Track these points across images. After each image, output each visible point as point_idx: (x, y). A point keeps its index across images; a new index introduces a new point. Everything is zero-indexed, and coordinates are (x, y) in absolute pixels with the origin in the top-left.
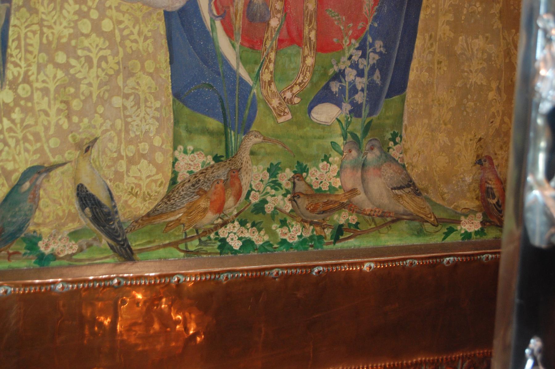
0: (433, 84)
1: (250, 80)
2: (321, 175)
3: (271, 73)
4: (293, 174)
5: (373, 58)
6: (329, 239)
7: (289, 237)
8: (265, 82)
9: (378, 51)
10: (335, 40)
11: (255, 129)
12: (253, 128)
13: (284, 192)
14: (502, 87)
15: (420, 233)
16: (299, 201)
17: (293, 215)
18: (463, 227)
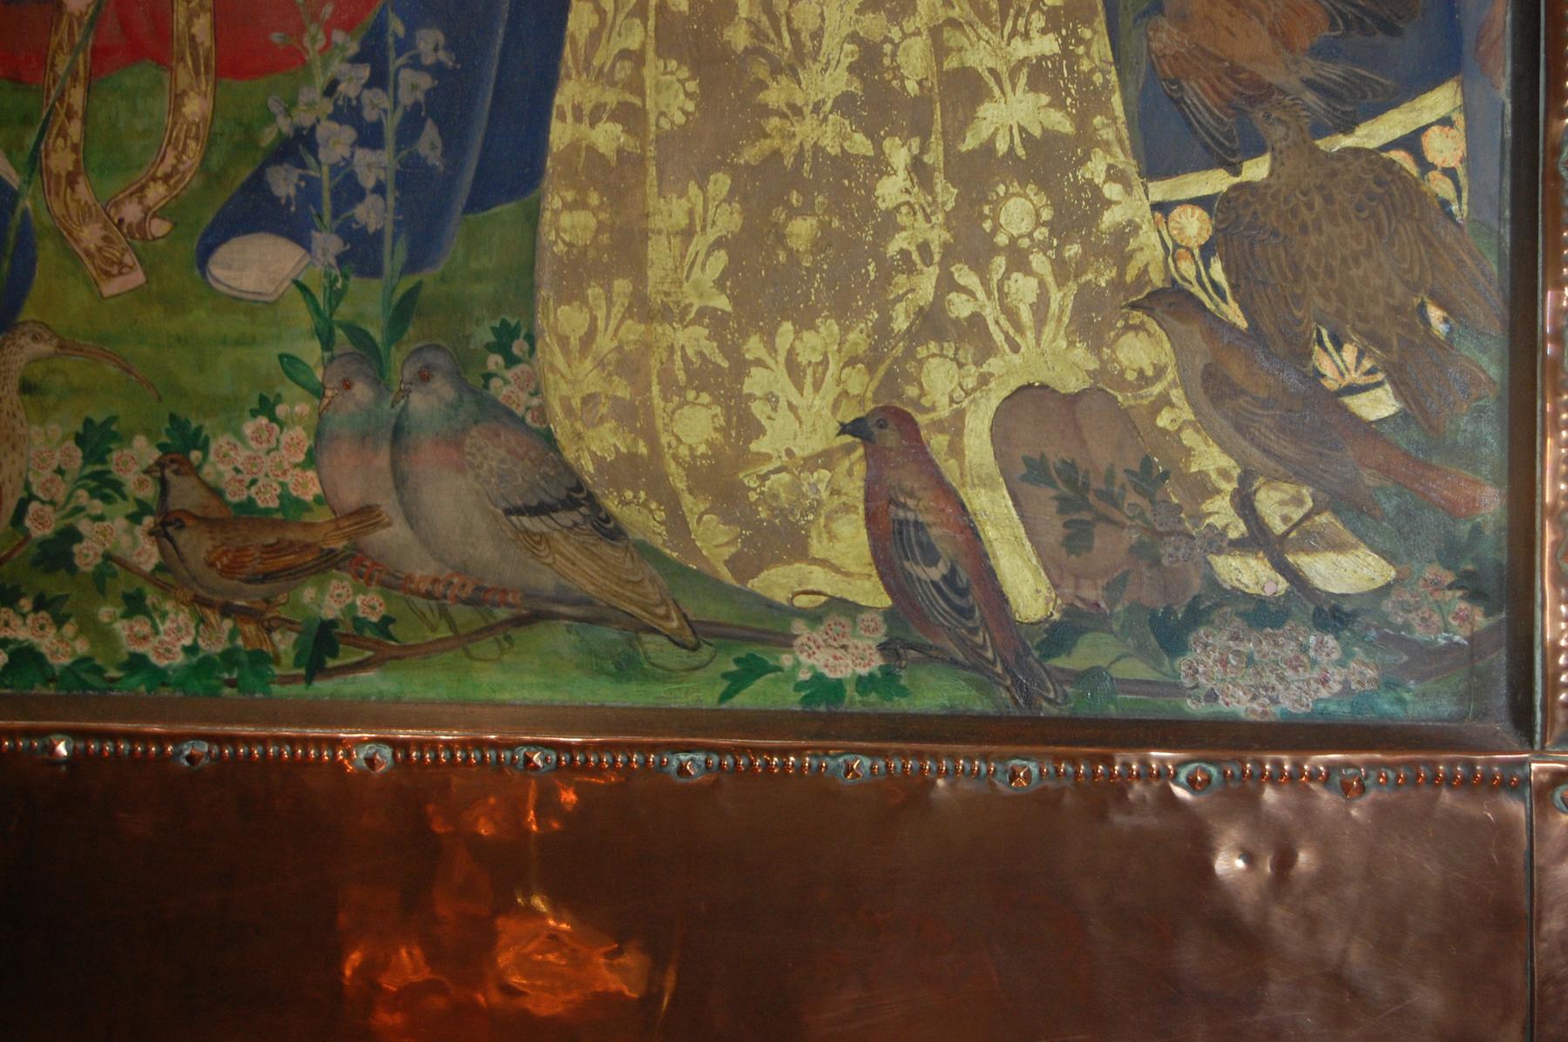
0: (642, 160)
1: (12, 171)
2: (252, 459)
3: (75, 148)
4: (157, 454)
5: (413, 85)
6: (287, 666)
7: (156, 650)
8: (58, 176)
9: (428, 60)
10: (276, 37)
11: (33, 316)
12: (28, 313)
13: (132, 508)
14: (935, 157)
15: (627, 667)
16: (182, 538)
17: (168, 576)
18: (803, 658)
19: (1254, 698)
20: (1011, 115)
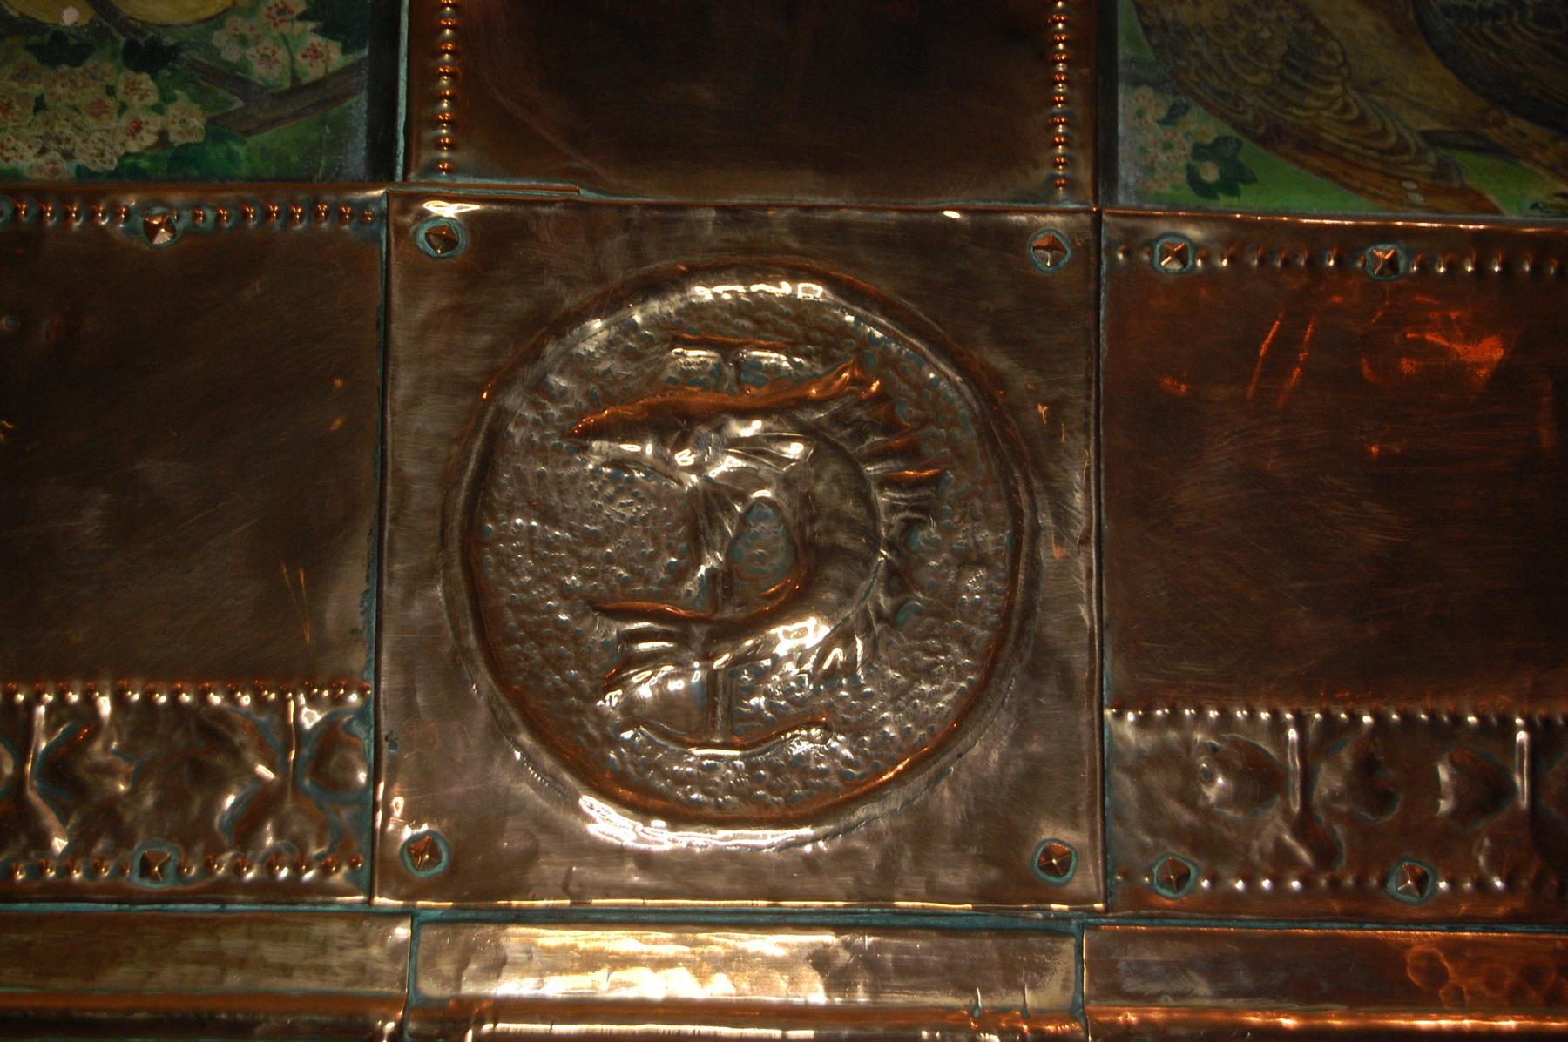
19: (43, 151)
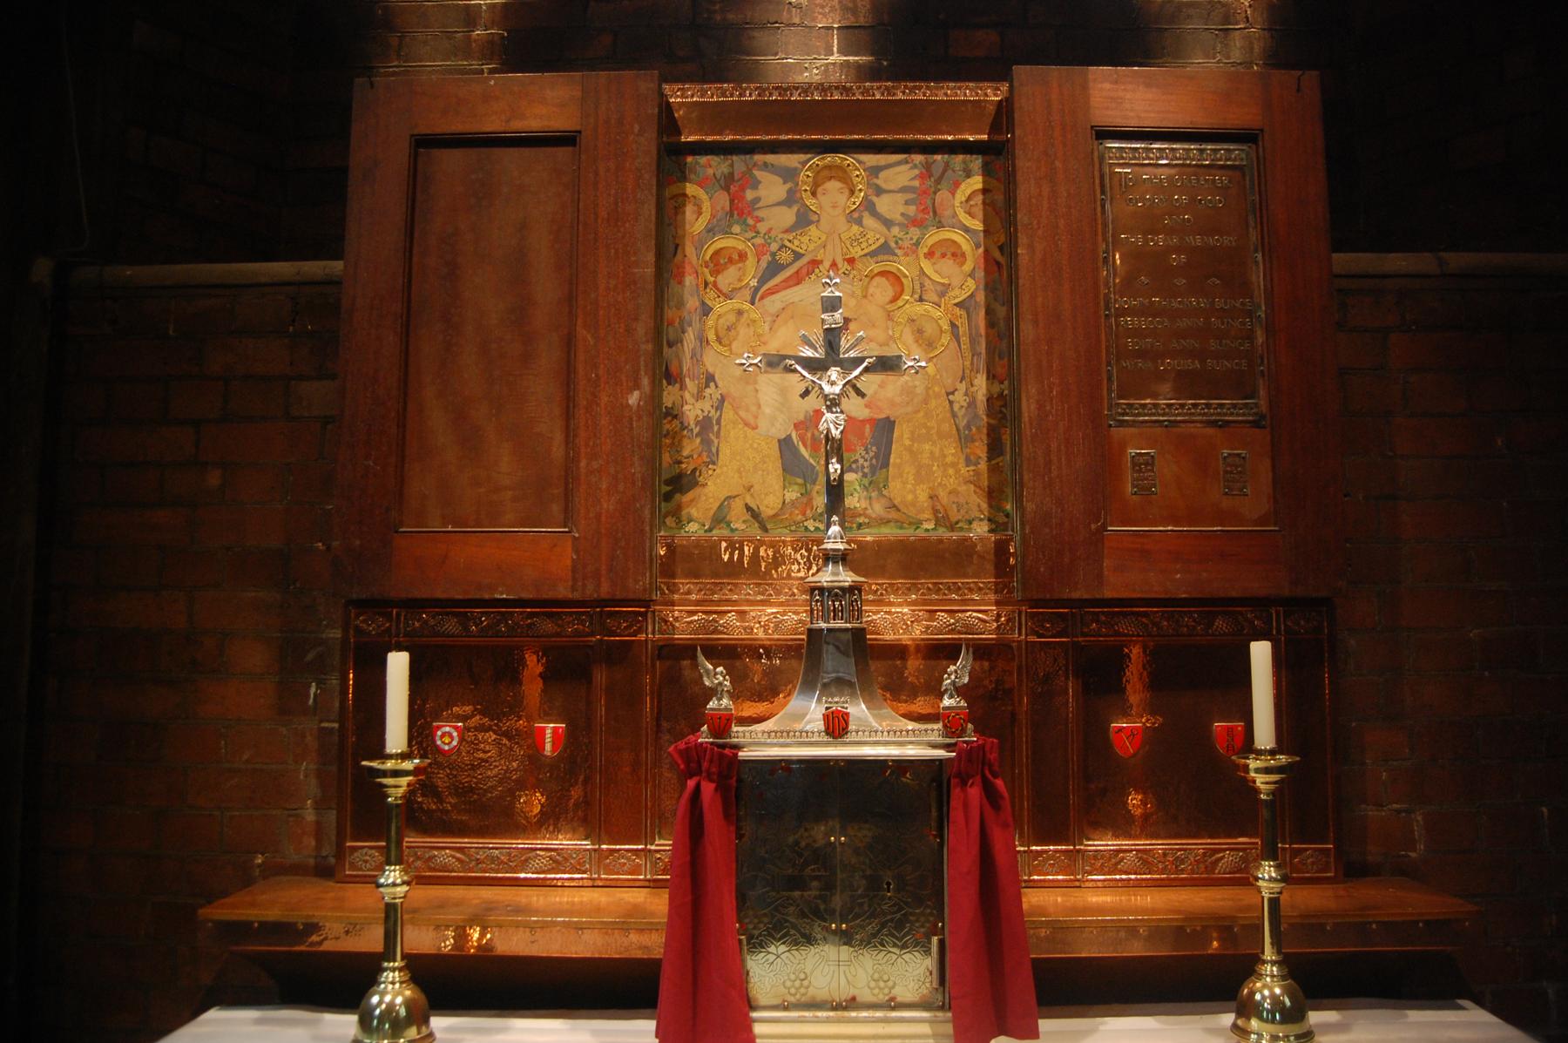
20: (949, 459)
